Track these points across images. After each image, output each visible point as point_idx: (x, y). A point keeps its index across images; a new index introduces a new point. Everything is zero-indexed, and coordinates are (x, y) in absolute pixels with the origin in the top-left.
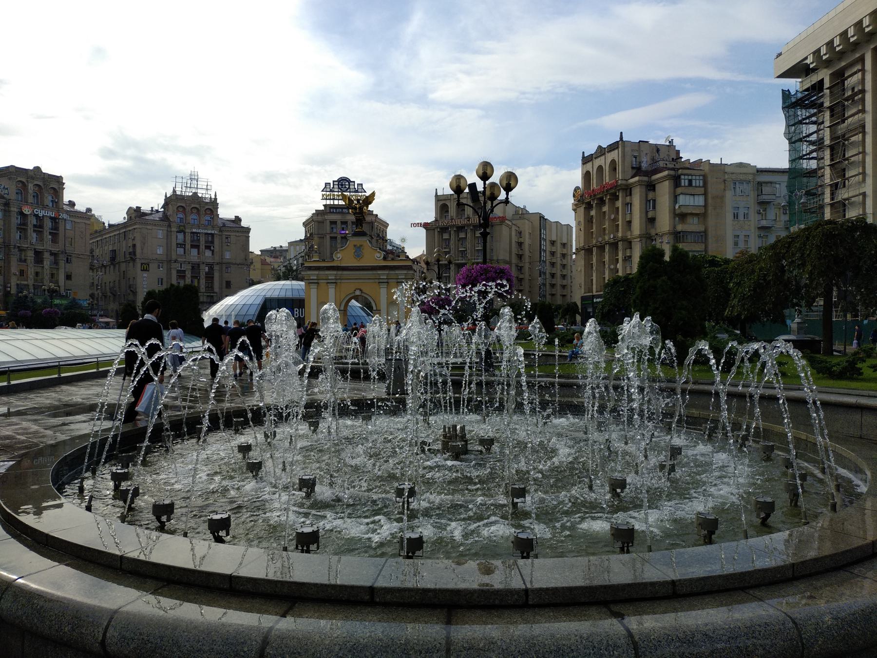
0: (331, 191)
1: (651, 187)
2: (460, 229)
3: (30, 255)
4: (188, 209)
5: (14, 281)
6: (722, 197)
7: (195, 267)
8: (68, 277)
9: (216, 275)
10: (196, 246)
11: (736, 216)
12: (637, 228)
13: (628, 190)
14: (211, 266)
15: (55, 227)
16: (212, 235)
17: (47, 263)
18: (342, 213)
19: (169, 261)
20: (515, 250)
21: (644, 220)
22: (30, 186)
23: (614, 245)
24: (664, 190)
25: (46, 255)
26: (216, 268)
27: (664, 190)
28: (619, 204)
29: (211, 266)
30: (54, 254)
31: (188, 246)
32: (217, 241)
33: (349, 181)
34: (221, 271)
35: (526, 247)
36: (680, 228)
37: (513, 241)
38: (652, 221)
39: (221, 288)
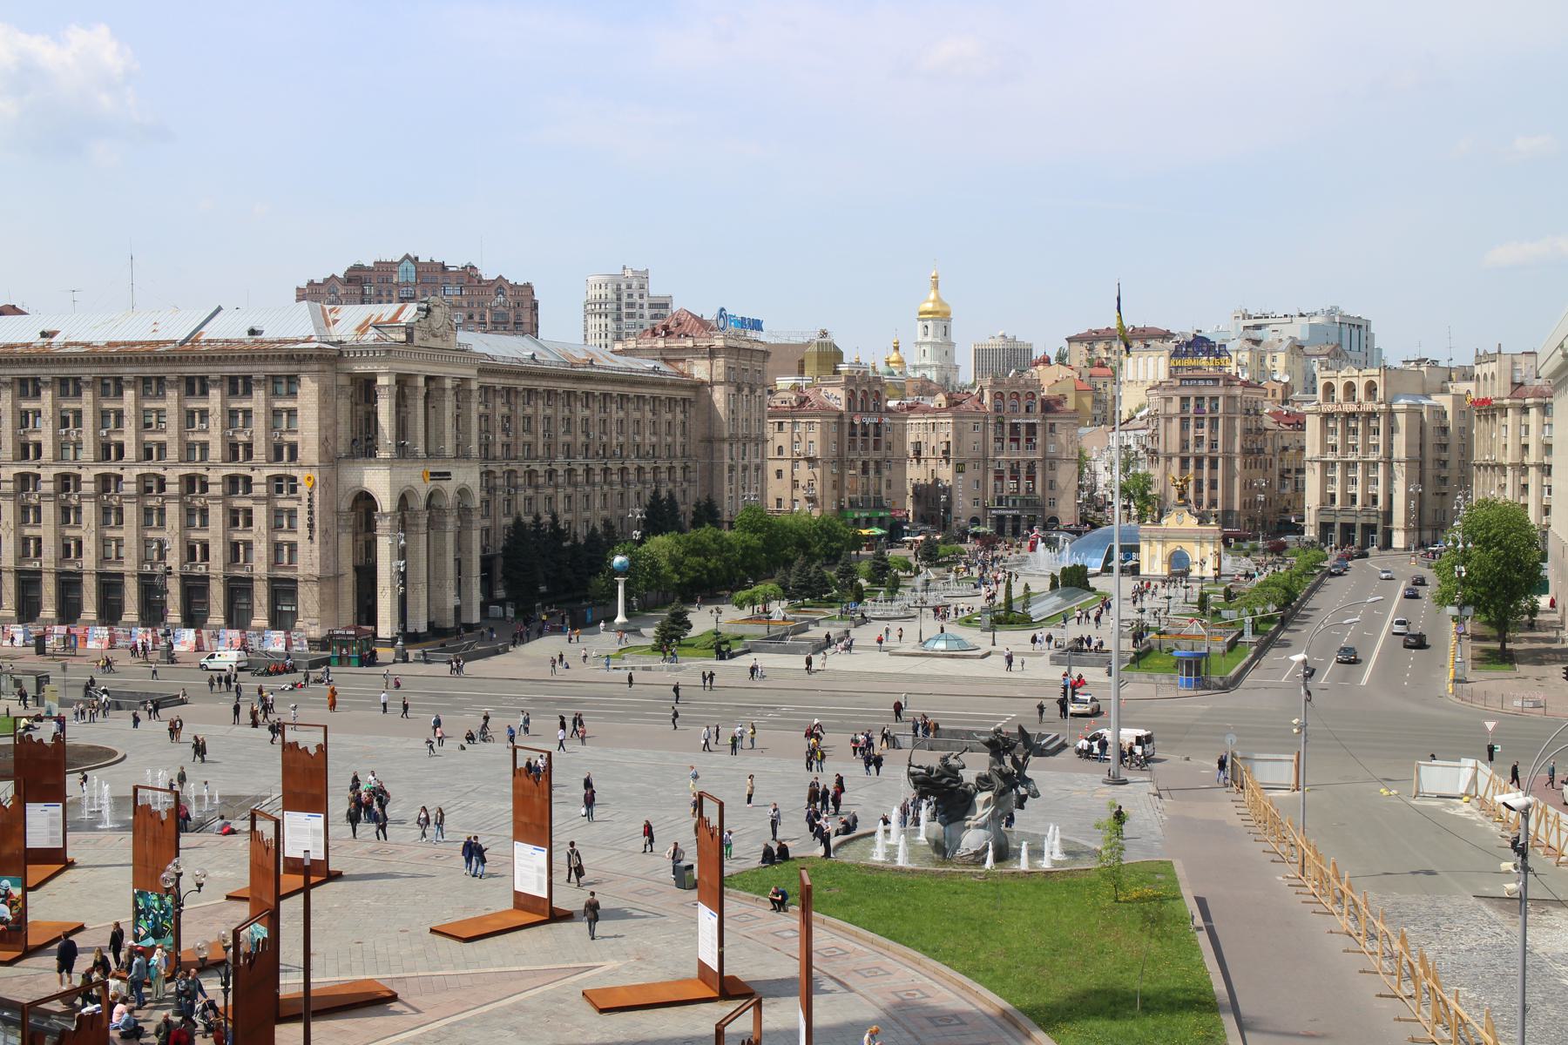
0: (1186, 355)
1: (1525, 410)
2: (1352, 415)
5: (847, 495)
8: (889, 486)
14: (1031, 466)
15: (878, 434)
16: (1034, 425)
17: (872, 472)
18: (1197, 386)
20: (1431, 438)
21: (1517, 447)
22: (859, 395)
25: (872, 465)
26: (1038, 465)
29: (1031, 466)
30: (877, 463)
31: (1007, 442)
32: (1039, 432)
34: (1044, 469)
38: (1526, 447)
39: (1044, 490)
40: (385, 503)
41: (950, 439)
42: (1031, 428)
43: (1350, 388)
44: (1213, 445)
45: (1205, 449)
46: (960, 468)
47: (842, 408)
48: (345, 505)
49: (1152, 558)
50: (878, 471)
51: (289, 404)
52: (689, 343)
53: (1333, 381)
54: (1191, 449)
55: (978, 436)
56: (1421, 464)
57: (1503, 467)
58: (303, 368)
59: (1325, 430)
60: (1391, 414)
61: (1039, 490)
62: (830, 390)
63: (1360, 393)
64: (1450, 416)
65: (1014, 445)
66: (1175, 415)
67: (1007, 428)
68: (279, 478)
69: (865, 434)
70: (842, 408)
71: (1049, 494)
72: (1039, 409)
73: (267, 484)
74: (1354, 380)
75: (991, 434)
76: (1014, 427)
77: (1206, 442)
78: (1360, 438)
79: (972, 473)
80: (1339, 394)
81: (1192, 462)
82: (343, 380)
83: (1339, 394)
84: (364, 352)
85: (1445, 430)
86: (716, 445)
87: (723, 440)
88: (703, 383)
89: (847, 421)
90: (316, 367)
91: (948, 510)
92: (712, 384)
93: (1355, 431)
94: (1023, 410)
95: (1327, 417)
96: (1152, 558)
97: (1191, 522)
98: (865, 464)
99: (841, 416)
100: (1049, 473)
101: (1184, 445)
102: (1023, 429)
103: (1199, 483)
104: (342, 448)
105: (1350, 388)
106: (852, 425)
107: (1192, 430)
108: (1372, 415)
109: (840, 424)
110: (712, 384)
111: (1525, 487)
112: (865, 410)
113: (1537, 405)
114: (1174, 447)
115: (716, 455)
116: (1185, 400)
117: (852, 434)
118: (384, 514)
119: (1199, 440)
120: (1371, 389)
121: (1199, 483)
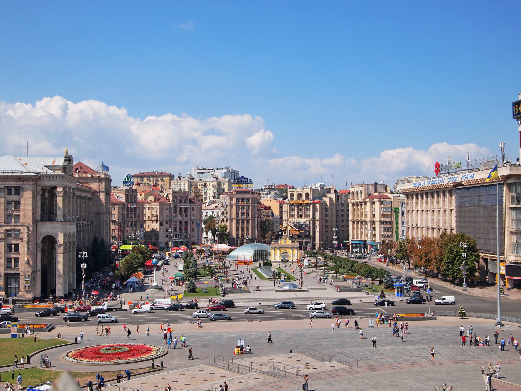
1: (374, 203)
2: (300, 205)
3: (130, 223)
4: (178, 197)
6: (398, 209)
7: (181, 222)
9: (189, 225)
10: (181, 213)
11: (402, 215)
12: (368, 219)
13: (366, 203)
17: (134, 226)
19: (171, 221)
23: (362, 222)
24: (377, 204)
26: (189, 223)
27: (377, 204)
28: (363, 206)
31: (178, 213)
32: (189, 211)
33: (245, 178)
35: (329, 210)
36: (382, 219)
37: (323, 209)
38: (374, 215)
40: (60, 239)
41: (158, 213)
42: (186, 209)
43: (300, 195)
44: (248, 215)
45: (245, 216)
46: (161, 224)
47: (124, 201)
48: (40, 241)
49: (275, 255)
50: (135, 225)
51: (15, 198)
52: (90, 176)
53: (294, 193)
54: (240, 217)
55: (168, 212)
56: (322, 221)
57: (366, 222)
58: (25, 183)
59: (292, 210)
60: (314, 205)
61: (189, 232)
62: (118, 195)
63: (304, 197)
64: (328, 205)
65: (180, 215)
66: (234, 204)
67: (178, 209)
68: (8, 230)
69: (131, 211)
70: (124, 201)
71: (192, 233)
72: (189, 202)
73: (5, 233)
74: (301, 193)
75: (173, 212)
76: (181, 208)
77: (245, 214)
78: (303, 212)
79: (166, 226)
80: (296, 197)
81: (241, 221)
82: (39, 189)
83: (296, 197)
84: (49, 177)
85: (327, 210)
86: (101, 216)
87: (104, 214)
88: (95, 191)
89: (126, 206)
90: (31, 183)
91: (157, 240)
92: (100, 192)
93: (301, 210)
94: (183, 201)
95: (291, 205)
96: (275, 255)
97: (289, 242)
98: (132, 222)
99: (124, 204)
100: (192, 225)
101: (238, 215)
102: (183, 210)
103: (243, 228)
104: (38, 217)
105: (300, 195)
106: (128, 207)
107: (240, 210)
108: (308, 204)
109: (124, 207)
110: (100, 192)
111: (374, 229)
112: (131, 202)
113: (379, 201)
114: (234, 216)
115: (101, 219)
116: (238, 199)
117: (128, 211)
118: (60, 245)
119: (243, 213)
120: (307, 195)
121: (243, 228)
